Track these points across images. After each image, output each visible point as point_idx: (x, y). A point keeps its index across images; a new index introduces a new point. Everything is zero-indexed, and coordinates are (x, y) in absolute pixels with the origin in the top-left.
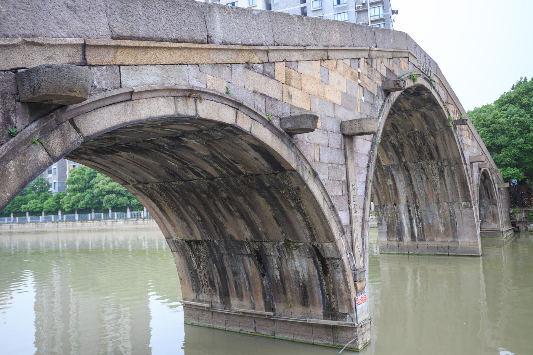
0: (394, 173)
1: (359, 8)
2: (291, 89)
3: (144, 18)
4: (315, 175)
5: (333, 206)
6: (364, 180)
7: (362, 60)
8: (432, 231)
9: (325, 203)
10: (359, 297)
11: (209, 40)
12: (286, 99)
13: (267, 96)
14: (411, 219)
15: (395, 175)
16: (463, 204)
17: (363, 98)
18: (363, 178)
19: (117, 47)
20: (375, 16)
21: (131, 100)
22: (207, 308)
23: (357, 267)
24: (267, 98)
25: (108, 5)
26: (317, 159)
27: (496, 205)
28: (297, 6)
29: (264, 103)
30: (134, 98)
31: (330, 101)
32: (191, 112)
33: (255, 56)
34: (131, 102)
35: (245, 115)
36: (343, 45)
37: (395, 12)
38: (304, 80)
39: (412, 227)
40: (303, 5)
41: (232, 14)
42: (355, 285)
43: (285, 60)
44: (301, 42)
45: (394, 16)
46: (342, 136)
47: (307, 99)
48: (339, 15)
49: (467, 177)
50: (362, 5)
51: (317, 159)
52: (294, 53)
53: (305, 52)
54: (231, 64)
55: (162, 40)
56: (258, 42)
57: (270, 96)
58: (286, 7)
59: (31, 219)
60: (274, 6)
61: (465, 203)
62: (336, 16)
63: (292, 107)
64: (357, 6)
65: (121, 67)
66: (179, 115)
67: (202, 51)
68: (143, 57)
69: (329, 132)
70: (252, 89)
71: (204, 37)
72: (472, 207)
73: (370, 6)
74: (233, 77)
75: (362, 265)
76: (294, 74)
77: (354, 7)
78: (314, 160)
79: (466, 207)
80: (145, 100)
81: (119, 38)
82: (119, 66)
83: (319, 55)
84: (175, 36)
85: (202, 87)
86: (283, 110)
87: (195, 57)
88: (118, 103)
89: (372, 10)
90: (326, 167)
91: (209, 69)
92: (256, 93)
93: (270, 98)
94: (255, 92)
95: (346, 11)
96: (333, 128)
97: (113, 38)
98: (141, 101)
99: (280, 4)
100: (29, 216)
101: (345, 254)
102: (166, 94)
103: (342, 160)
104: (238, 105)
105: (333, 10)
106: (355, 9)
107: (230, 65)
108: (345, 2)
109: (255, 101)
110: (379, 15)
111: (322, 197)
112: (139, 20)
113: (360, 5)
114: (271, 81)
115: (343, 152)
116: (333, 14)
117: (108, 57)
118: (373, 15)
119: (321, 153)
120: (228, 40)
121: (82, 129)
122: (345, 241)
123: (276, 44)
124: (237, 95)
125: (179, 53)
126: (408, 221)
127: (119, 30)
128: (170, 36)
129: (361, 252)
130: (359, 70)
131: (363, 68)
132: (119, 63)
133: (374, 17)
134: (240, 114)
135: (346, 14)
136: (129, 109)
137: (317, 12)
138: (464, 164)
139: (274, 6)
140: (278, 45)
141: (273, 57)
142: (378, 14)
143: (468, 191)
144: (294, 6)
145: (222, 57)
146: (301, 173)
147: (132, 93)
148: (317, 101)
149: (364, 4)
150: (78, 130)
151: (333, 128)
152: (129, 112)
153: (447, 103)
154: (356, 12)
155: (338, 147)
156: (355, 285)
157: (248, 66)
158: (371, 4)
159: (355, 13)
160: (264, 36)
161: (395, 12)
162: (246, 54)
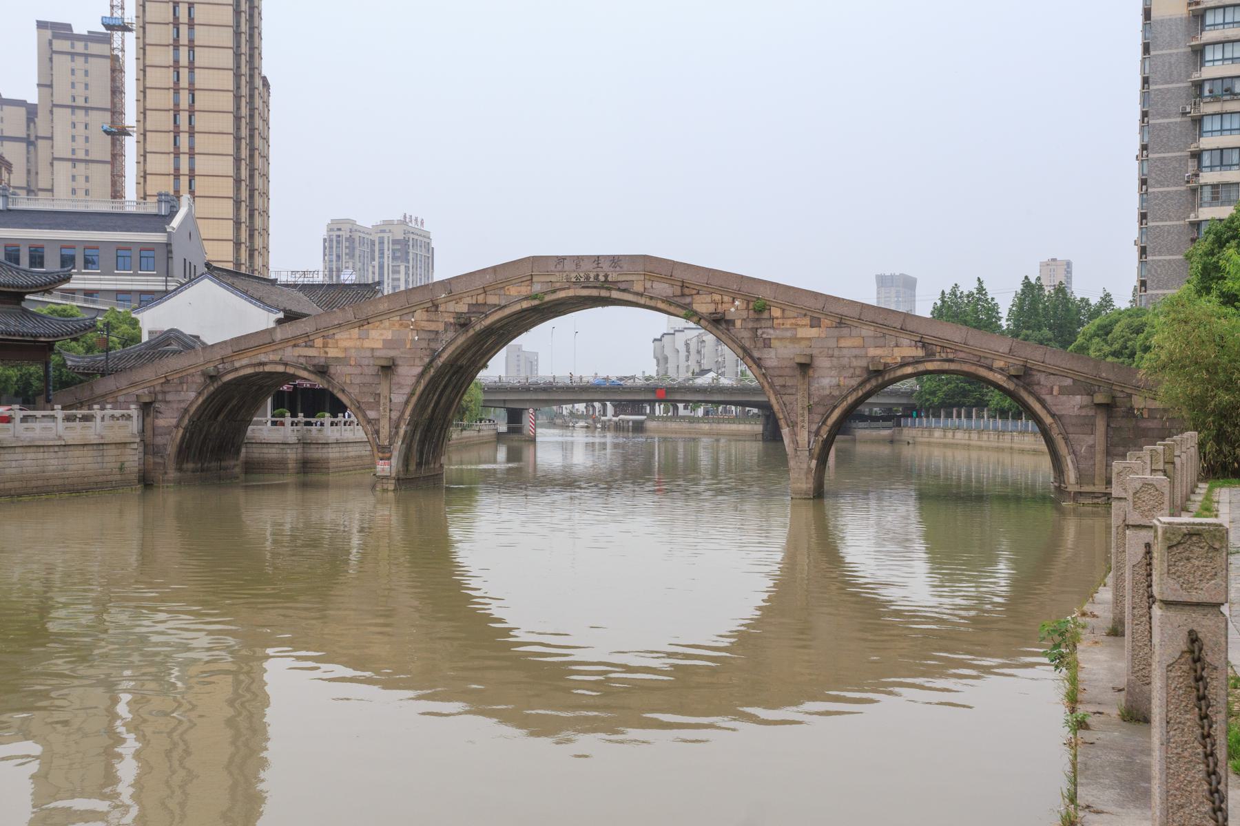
2: (327, 349)
4: (343, 391)
12: (323, 355)
17: (416, 338)
18: (407, 390)
26: (348, 381)
32: (261, 370)
68: (242, 356)
71: (270, 341)
75: (386, 443)
78: (345, 383)
83: (358, 324)
85: (266, 360)
104: (286, 364)
114: (311, 349)
117: (230, 359)
124: (285, 359)
130: (413, 320)
131: (420, 315)
134: (288, 367)
141: (311, 338)
145: (280, 346)
146: (330, 389)
153: (683, 295)
157: (295, 346)
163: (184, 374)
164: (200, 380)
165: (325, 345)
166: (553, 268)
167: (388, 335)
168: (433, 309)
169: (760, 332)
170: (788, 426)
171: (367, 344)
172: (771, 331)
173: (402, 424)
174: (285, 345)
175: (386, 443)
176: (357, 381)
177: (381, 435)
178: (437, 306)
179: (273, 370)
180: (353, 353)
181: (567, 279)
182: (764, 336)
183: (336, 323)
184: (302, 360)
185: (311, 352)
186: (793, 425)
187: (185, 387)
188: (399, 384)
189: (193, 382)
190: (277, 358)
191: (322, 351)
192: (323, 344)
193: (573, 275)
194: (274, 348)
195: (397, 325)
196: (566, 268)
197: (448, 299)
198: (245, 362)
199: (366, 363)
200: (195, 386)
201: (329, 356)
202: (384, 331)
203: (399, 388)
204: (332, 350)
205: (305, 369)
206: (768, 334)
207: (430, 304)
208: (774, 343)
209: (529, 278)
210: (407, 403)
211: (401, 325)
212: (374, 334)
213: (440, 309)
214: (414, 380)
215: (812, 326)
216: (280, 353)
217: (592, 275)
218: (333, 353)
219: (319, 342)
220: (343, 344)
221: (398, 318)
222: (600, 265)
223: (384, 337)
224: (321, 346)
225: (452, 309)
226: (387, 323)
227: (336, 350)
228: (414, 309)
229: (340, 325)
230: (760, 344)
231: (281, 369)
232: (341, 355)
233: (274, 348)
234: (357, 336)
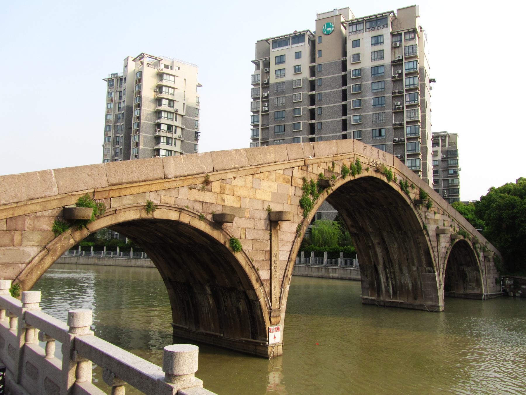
0: (372, 238)
1: (395, 77)
2: (224, 196)
3: (126, 173)
5: (254, 267)
6: (289, 249)
7: (296, 168)
8: (403, 290)
9: (247, 265)
10: (273, 327)
11: (165, 176)
12: (220, 202)
13: (204, 202)
14: (387, 279)
15: (373, 240)
16: (427, 269)
19: (110, 190)
20: (409, 85)
21: (115, 213)
22: (186, 329)
23: (272, 307)
24: (204, 204)
25: (108, 171)
26: (243, 237)
27: (479, 271)
28: (338, 73)
29: (201, 206)
30: (117, 212)
31: (259, 200)
33: (197, 180)
34: (115, 214)
35: (186, 215)
36: (277, 160)
37: (432, 81)
38: (236, 189)
39: (388, 286)
40: (343, 73)
41: (182, 160)
42: (270, 319)
43: (221, 179)
44: (237, 166)
45: (432, 83)
46: (269, 221)
47: (238, 200)
48: (376, 84)
49: (430, 246)
50: (398, 75)
51: (243, 237)
52: (229, 174)
53: (238, 172)
54: (179, 187)
55: (136, 182)
56: (201, 171)
57: (206, 202)
58: (329, 74)
59: (94, 253)
60: (318, 74)
61: (429, 268)
62: (373, 84)
63: (224, 206)
64: (393, 76)
65: (112, 198)
66: (142, 218)
67: (159, 184)
69: (256, 220)
70: (193, 199)
72: (434, 272)
73: (406, 76)
74: (179, 194)
75: (277, 306)
76: (228, 186)
77: (391, 77)
79: (429, 272)
80: (123, 213)
81: (113, 185)
82: (111, 198)
83: (252, 172)
84: (143, 178)
86: (216, 209)
87: (154, 188)
88: (109, 215)
89: (407, 80)
90: (251, 242)
91: (163, 192)
92: (196, 201)
93: (206, 203)
94: (195, 201)
95: (383, 80)
96: (260, 217)
97: (109, 185)
98: (121, 213)
99: (323, 71)
100: (93, 250)
101: (263, 298)
102: (135, 208)
103: (268, 237)
105: (370, 79)
106: (390, 79)
107: (178, 188)
108: (383, 71)
109: (195, 206)
110: (414, 84)
111: (245, 261)
112: (124, 174)
113: (396, 75)
115: (269, 232)
116: (370, 82)
118: (408, 84)
119: (247, 233)
120: (178, 174)
121: (90, 229)
122: (263, 290)
123: (215, 170)
125: (144, 187)
126: (385, 280)
127: (112, 181)
128: (141, 179)
129: (277, 298)
132: (111, 197)
133: (408, 86)
134: (182, 214)
135: (383, 83)
136: (114, 217)
137: (357, 80)
138: (426, 236)
139: (318, 74)
140: (217, 171)
142: (413, 83)
143: (431, 258)
144: (336, 74)
145: (174, 184)
147: (116, 210)
148: (247, 200)
149: (399, 74)
150: (88, 229)
151: (260, 217)
152: (114, 219)
154: (392, 81)
155: (264, 228)
156: (270, 319)
158: (406, 74)
159: (391, 82)
160: (205, 167)
161: (432, 81)
162: (190, 180)
163: (18, 212)
164: (47, 225)
165: (222, 191)
166: (362, 153)
167: (275, 188)
168: (305, 168)
169: (426, 213)
170: (437, 271)
171: (260, 195)
172: (429, 213)
173: (286, 283)
174: (180, 183)
175: (277, 306)
176: (250, 236)
177: (273, 297)
178: (307, 167)
179: (165, 217)
180: (246, 204)
181: (369, 163)
182: (428, 217)
183: (233, 166)
184: (198, 207)
185: (207, 197)
186: (439, 270)
187: (17, 238)
188: (282, 241)
189: (34, 230)
190: (171, 201)
191: (219, 198)
192: (221, 189)
193: (372, 160)
194: (167, 185)
195: (281, 179)
196: (367, 154)
197: (315, 161)
198: (127, 201)
199: (258, 217)
200: (37, 237)
201: (226, 204)
202: (272, 184)
203: (284, 245)
204: (228, 197)
205: (201, 218)
206: (429, 216)
207: (302, 163)
208: (430, 221)
209: (352, 156)
210: (289, 260)
211: (284, 179)
212: (265, 184)
213: (310, 169)
214: (294, 235)
215: (438, 214)
216: (174, 193)
217: (378, 164)
218: (230, 201)
219: (216, 186)
220: (239, 192)
221: (281, 172)
222: (379, 157)
223: (272, 190)
224: (219, 191)
225: (315, 172)
226: (273, 176)
227: (232, 198)
228: (293, 165)
229: (236, 169)
230: (427, 222)
231: (173, 216)
232: (236, 205)
233: (167, 185)
234: (249, 185)
